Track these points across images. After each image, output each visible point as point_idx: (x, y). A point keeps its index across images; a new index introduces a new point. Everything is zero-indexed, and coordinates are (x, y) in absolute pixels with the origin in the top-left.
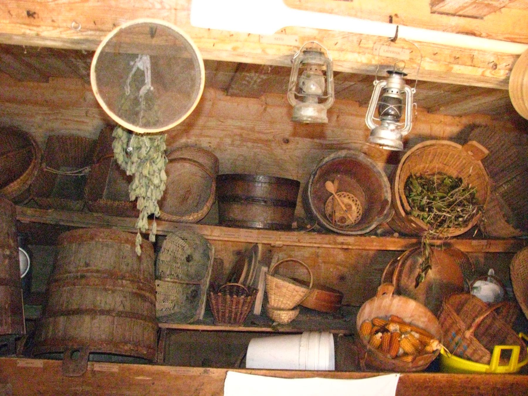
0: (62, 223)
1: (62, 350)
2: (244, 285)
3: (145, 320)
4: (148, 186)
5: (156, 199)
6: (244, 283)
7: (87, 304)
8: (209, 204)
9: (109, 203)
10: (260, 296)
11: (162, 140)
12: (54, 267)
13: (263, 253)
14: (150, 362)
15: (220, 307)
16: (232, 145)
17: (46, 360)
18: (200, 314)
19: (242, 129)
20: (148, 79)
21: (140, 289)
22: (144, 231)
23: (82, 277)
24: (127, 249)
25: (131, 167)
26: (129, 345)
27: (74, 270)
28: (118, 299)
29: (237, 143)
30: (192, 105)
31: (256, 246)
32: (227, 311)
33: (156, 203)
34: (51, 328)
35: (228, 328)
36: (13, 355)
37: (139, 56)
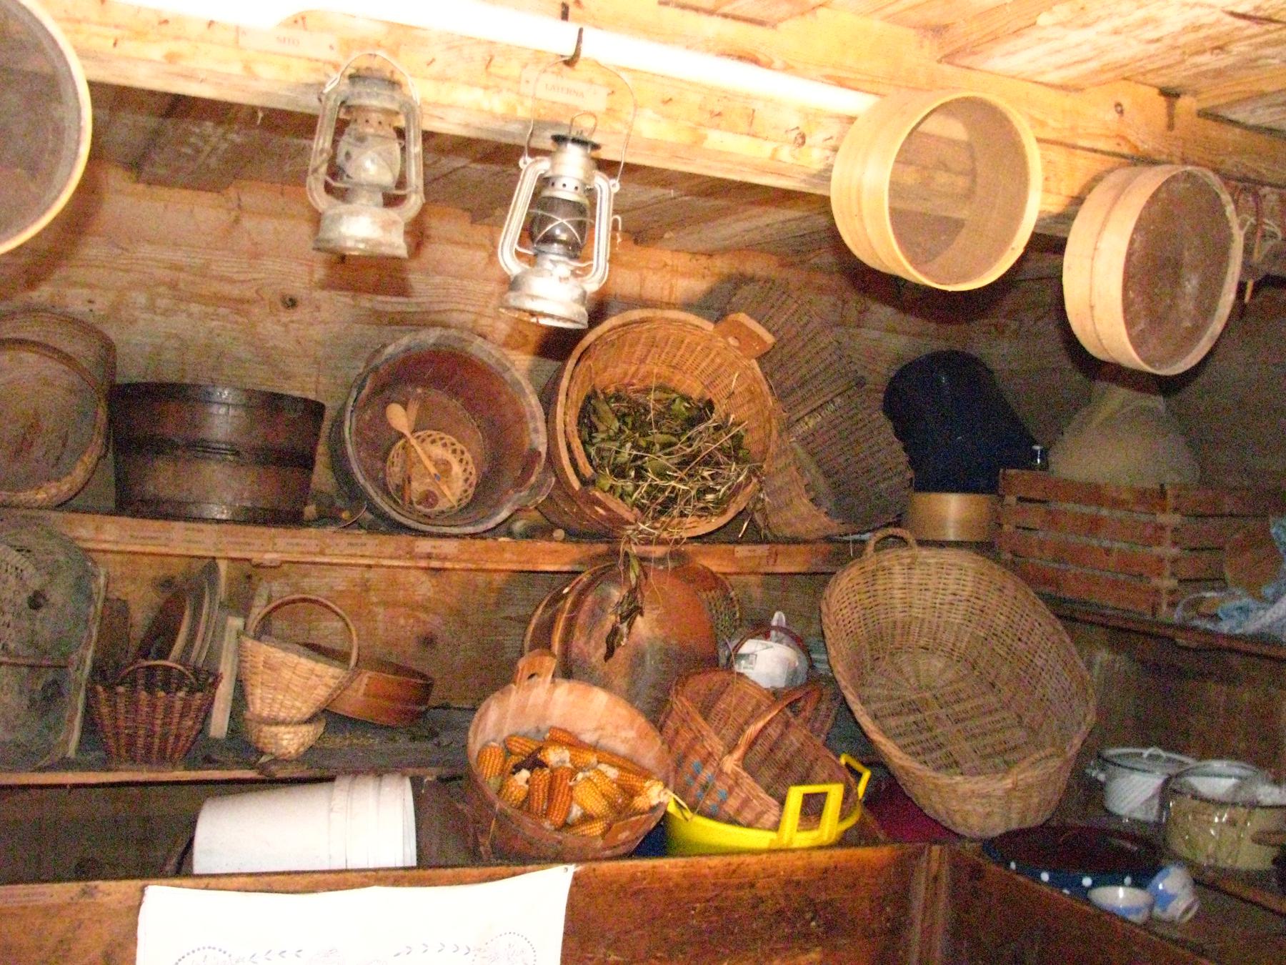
2: (184, 665)
8: (89, 459)
10: (225, 691)
13: (231, 581)
15: (121, 723)
16: (151, 308)
18: (67, 743)
29: (162, 303)
30: (56, 198)
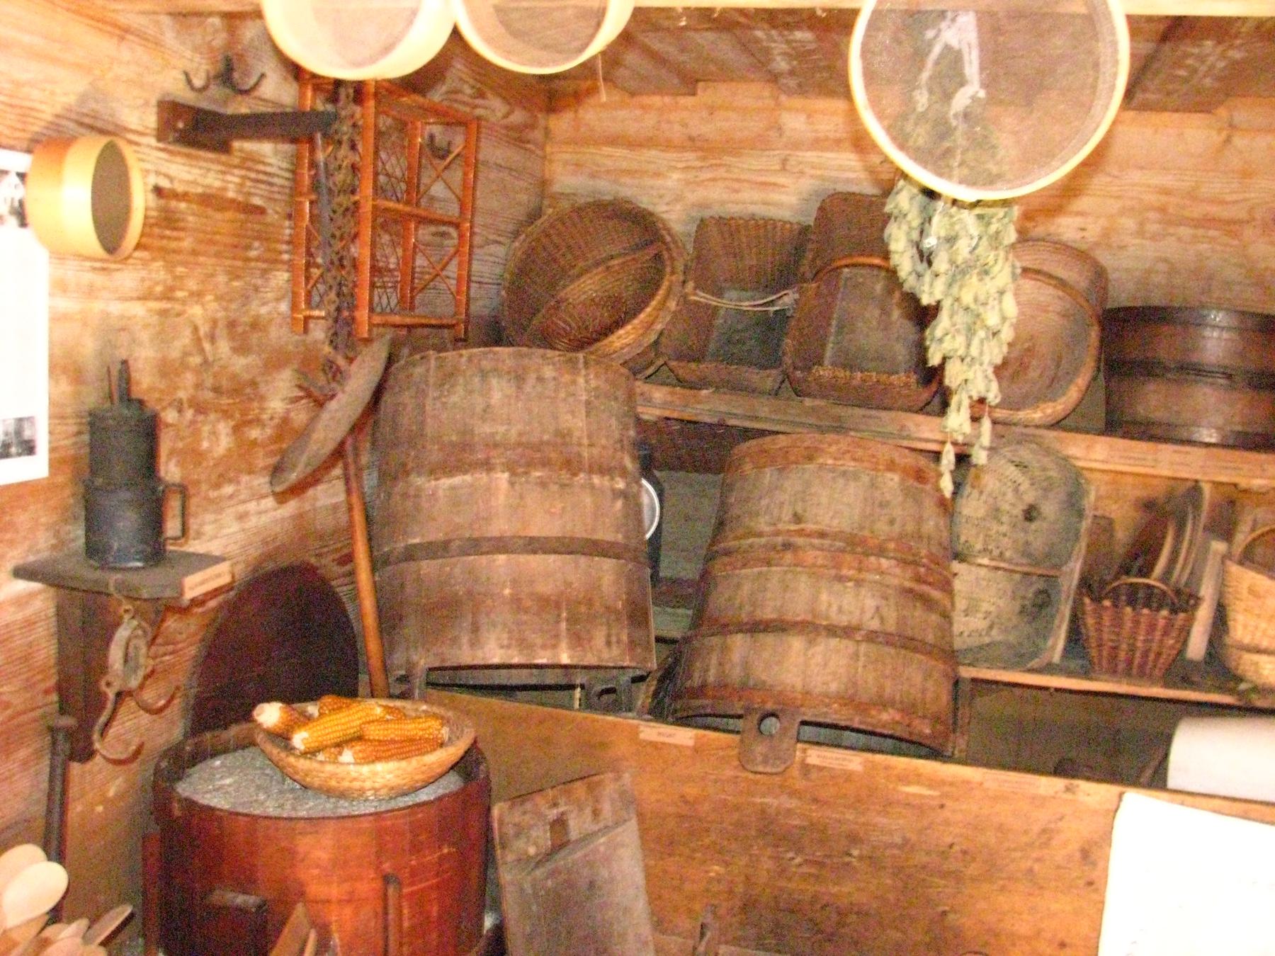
0: (732, 422)
1: (740, 712)
2: (1167, 584)
3: (929, 653)
4: (970, 332)
5: (990, 363)
6: (1165, 577)
7: (797, 609)
8: (1082, 381)
9: (841, 374)
10: (1204, 614)
11: (1006, 220)
12: (721, 524)
13: (1213, 506)
14: (935, 754)
15: (1106, 636)
16: (1141, 233)
17: (701, 732)
18: (1053, 647)
19: (1166, 192)
20: (972, 68)
21: (919, 579)
22: (960, 439)
23: (787, 546)
24: (891, 484)
25: (931, 285)
26: (891, 711)
27: (767, 529)
28: (870, 603)
29: (1153, 228)
30: (1095, 130)
31: (1195, 488)
32: (1124, 646)
33: (990, 371)
34: (714, 661)
35: (1123, 688)
36: (630, 714)
37: (949, 15)
